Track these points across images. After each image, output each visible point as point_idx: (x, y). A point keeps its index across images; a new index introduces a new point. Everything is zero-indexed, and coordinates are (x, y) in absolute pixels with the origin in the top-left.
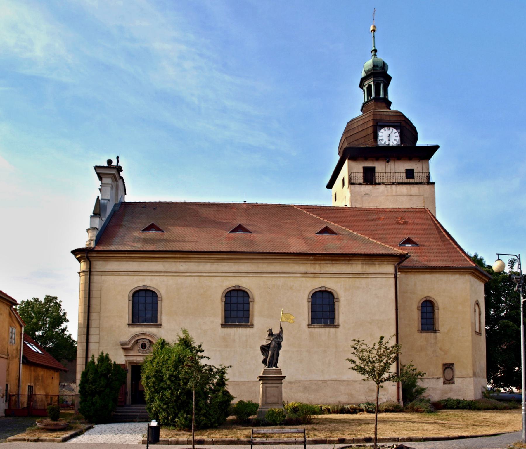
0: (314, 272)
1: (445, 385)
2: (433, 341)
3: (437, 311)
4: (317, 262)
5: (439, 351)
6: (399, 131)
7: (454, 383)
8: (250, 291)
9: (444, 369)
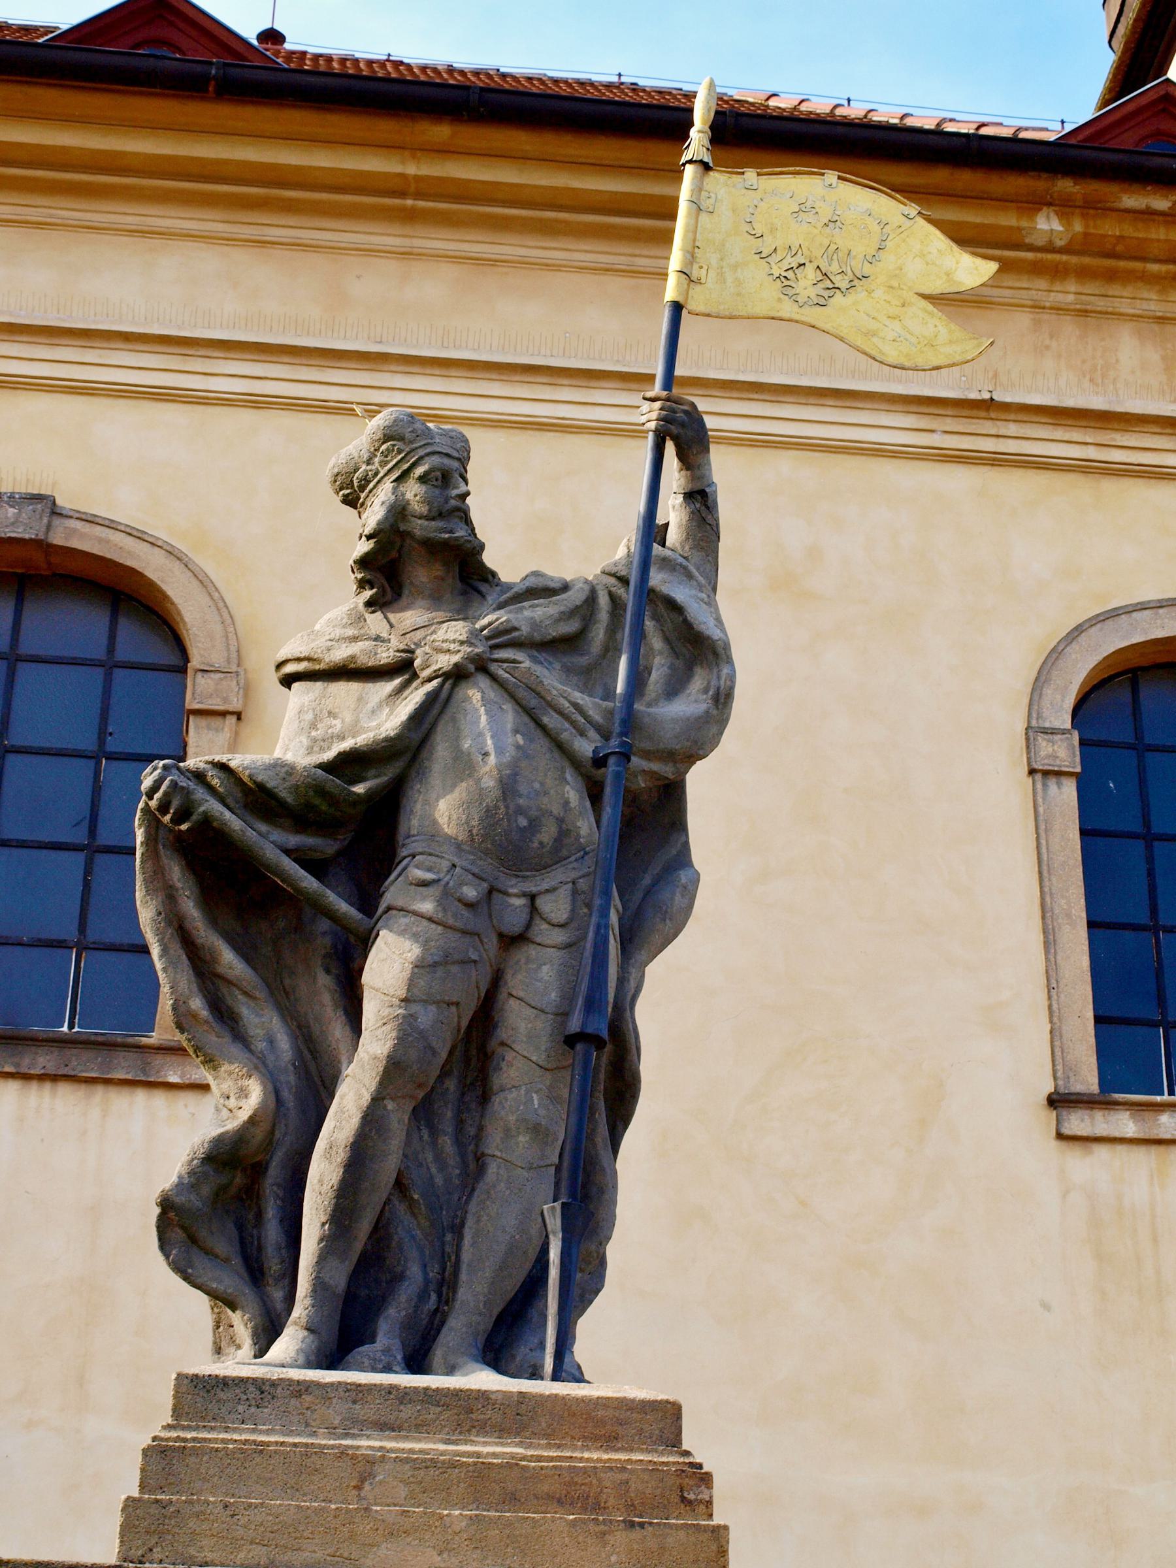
0: (1097, 403)
4: (1125, 299)
8: (203, 581)
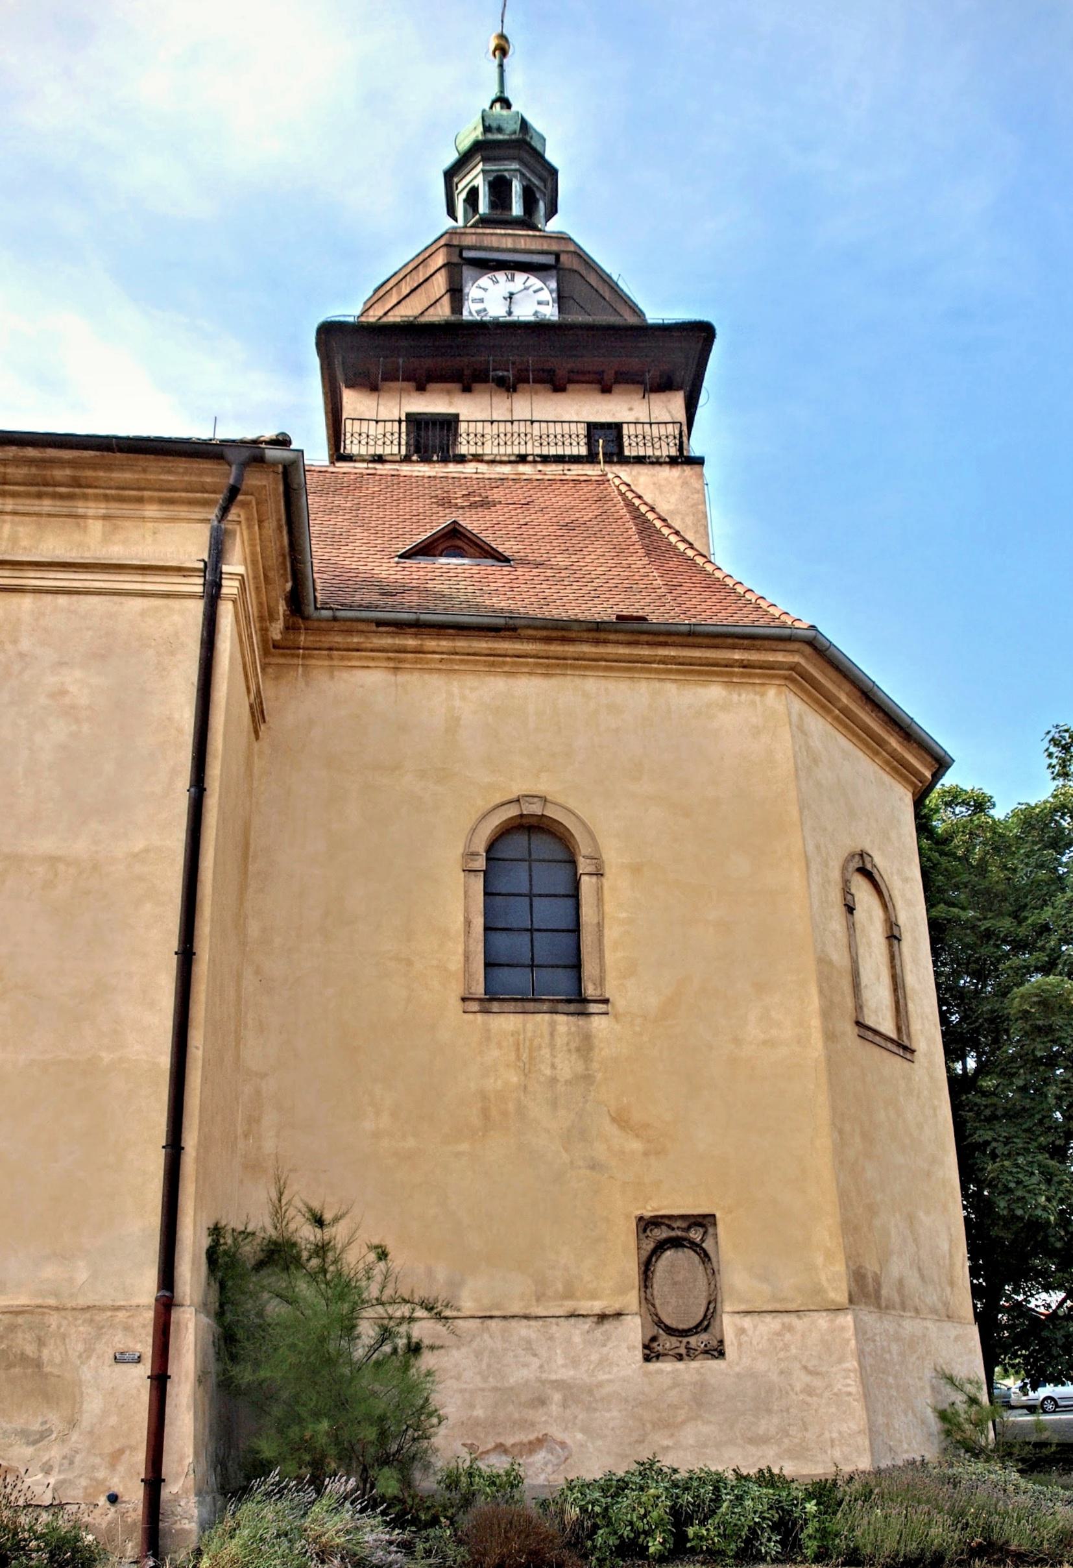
1: (653, 1366)
2: (567, 1066)
3: (594, 879)
5: (611, 1129)
6: (553, 285)
7: (718, 1352)
9: (645, 1255)
